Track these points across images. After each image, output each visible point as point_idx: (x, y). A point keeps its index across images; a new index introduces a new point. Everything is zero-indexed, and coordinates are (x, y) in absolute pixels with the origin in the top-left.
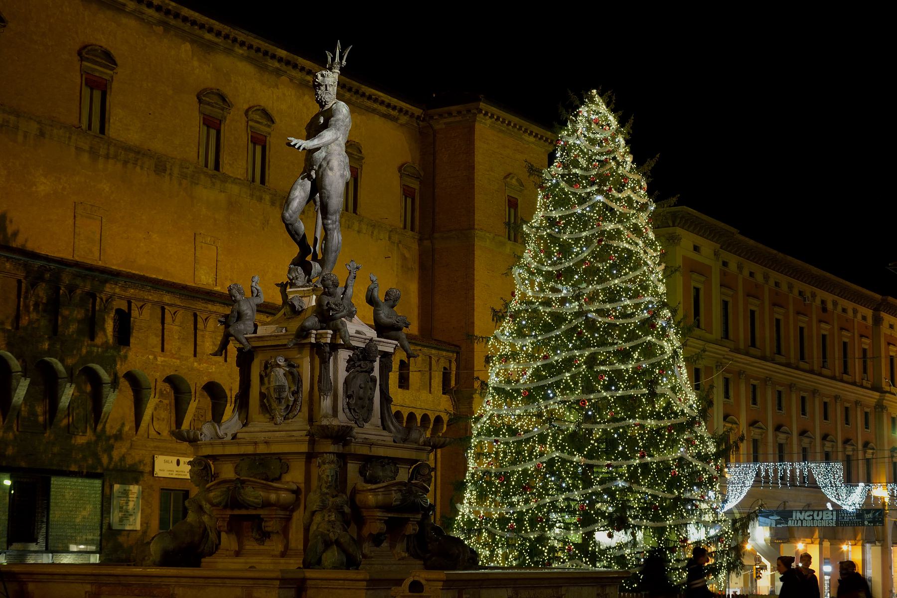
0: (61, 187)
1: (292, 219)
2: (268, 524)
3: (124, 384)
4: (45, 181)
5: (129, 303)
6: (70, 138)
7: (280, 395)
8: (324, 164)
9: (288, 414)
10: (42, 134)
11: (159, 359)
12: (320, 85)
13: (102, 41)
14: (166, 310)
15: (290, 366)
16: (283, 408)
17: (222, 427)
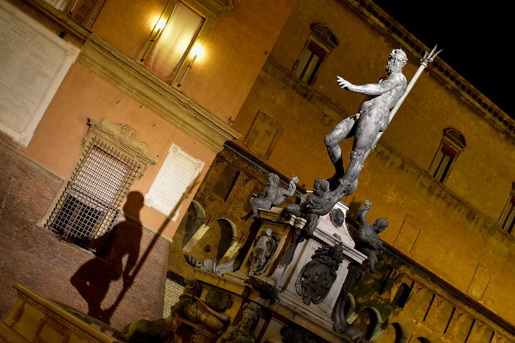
0: (402, 202)
1: (331, 143)
2: (196, 336)
3: (393, 331)
4: (393, 195)
5: (413, 283)
6: (419, 176)
7: (257, 256)
8: (367, 111)
9: (257, 271)
10: (402, 167)
11: (419, 324)
12: (391, 58)
13: (462, 129)
14: (435, 297)
15: (273, 237)
16: (256, 266)
17: (219, 267)
